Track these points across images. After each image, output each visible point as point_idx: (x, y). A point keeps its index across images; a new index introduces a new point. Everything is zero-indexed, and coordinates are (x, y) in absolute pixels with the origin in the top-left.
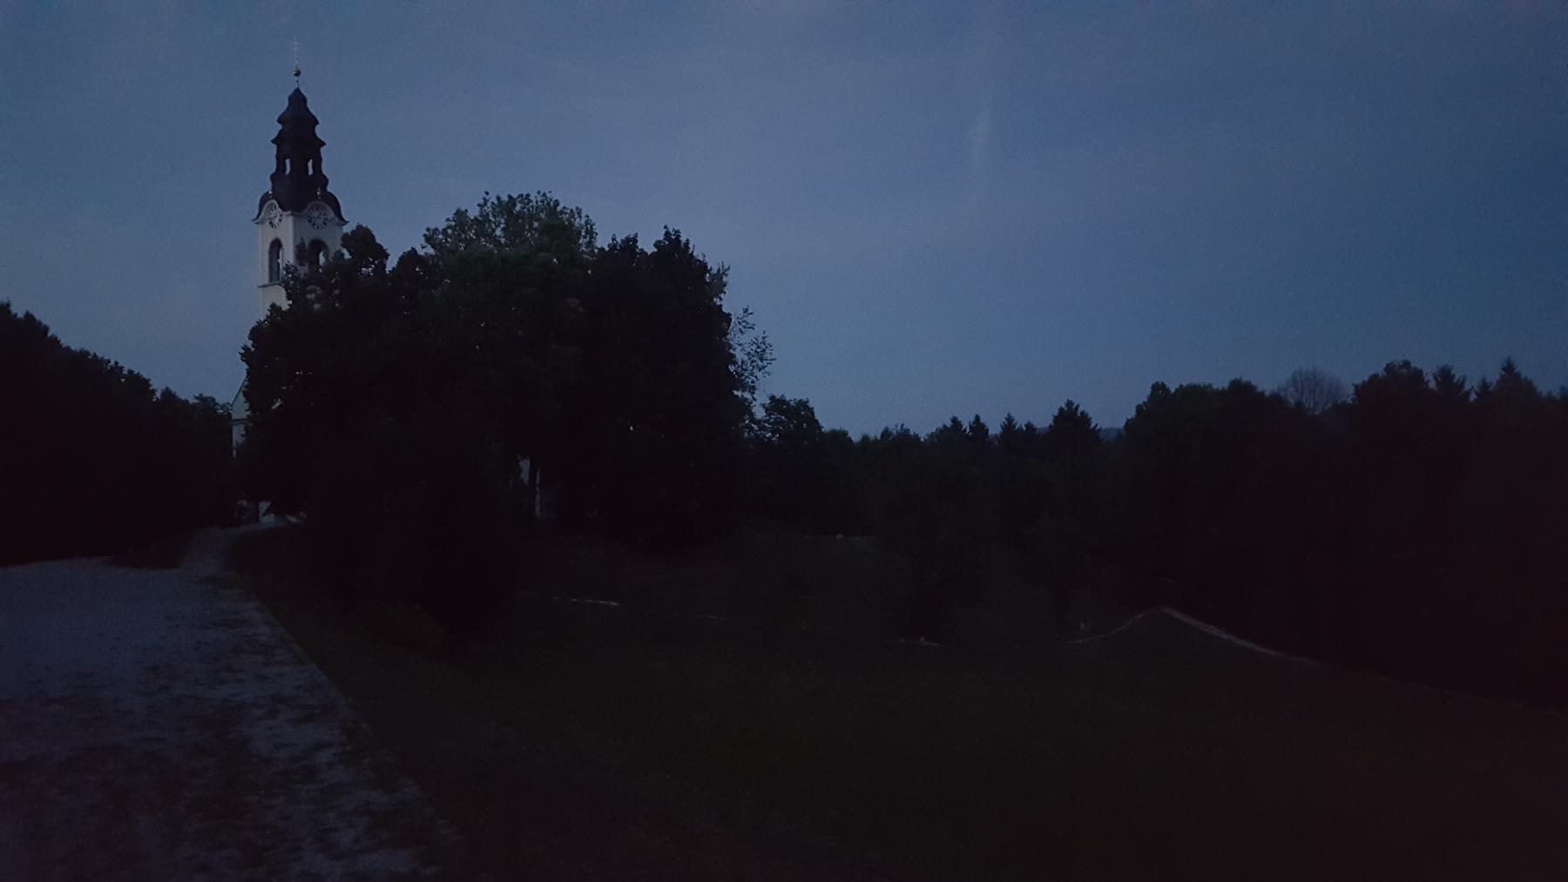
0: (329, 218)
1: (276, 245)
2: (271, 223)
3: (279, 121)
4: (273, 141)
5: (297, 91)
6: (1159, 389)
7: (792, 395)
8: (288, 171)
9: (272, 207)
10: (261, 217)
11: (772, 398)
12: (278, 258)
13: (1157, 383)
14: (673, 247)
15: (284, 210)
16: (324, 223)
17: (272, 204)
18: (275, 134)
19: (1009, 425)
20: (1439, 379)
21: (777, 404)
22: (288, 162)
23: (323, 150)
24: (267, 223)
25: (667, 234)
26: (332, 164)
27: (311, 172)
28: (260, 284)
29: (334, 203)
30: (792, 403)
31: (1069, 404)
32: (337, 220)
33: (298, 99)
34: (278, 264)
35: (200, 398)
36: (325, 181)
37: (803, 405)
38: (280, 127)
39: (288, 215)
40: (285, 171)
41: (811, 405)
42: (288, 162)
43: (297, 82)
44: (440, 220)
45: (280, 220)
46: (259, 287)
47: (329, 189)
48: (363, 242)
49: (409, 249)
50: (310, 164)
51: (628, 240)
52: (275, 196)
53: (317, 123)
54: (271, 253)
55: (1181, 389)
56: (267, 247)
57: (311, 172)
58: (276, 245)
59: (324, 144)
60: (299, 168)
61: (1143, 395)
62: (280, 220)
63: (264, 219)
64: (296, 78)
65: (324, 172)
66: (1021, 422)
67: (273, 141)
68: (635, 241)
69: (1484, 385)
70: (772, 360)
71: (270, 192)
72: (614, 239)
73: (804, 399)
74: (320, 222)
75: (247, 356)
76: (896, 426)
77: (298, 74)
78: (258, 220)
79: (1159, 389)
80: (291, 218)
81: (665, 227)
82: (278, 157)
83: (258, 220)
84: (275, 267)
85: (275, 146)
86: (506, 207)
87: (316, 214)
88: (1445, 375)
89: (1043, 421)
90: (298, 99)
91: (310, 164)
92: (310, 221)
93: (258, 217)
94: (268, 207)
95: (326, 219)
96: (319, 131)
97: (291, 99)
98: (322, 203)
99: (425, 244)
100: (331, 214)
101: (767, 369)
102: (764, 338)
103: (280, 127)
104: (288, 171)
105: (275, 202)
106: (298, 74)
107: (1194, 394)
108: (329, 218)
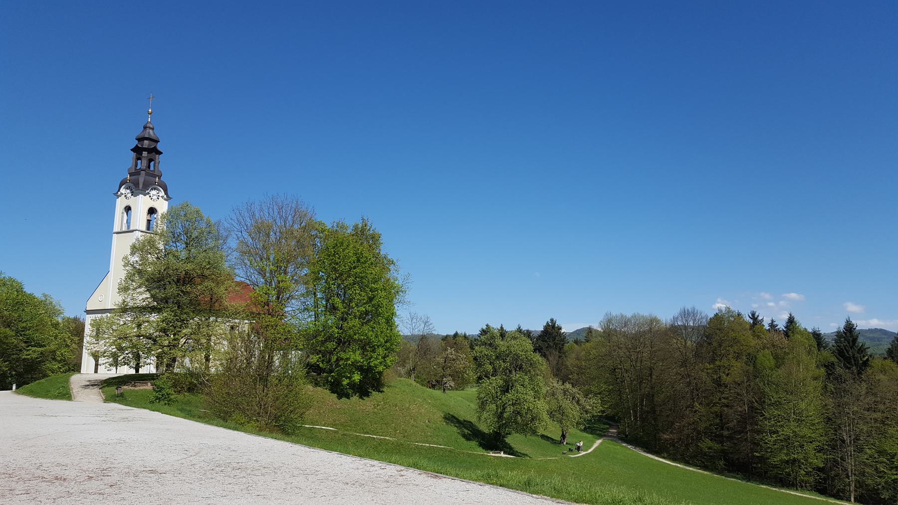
2: (125, 196)
3: (136, 139)
4: (132, 150)
10: (119, 193)
16: (158, 198)
18: (133, 146)
19: (519, 330)
20: (751, 316)
26: (163, 164)
27: (152, 168)
28: (116, 229)
31: (552, 320)
32: (165, 196)
40: (136, 166)
45: (132, 195)
46: (114, 233)
47: (162, 179)
50: (152, 164)
58: (128, 209)
59: (161, 153)
65: (162, 167)
66: (524, 328)
67: (132, 150)
69: (773, 321)
74: (155, 197)
87: (154, 192)
88: (754, 316)
89: (538, 327)
92: (150, 196)
95: (159, 196)
96: (159, 147)
97: (145, 128)
100: (163, 193)
105: (131, 185)
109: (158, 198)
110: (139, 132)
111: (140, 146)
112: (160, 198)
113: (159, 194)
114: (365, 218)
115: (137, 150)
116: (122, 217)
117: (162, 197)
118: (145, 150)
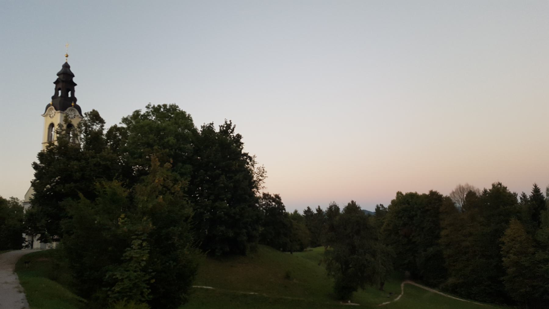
0: (76, 115)
1: (52, 125)
2: (50, 116)
3: (58, 75)
4: (55, 83)
5: (66, 63)
6: (399, 194)
7: (272, 194)
8: (60, 94)
9: (51, 109)
10: (46, 114)
11: (264, 194)
12: (52, 131)
13: (399, 192)
14: (227, 128)
15: (56, 109)
17: (52, 108)
18: (55, 80)
21: (266, 196)
22: (60, 92)
23: (76, 87)
24: (48, 116)
25: (226, 122)
26: (79, 92)
27: (70, 96)
29: (79, 109)
30: (272, 196)
32: (80, 116)
33: (66, 66)
34: (52, 134)
35: (12, 198)
36: (74, 99)
37: (277, 196)
38: (58, 77)
39: (58, 113)
41: (280, 196)
42: (60, 92)
43: (67, 59)
44: (129, 113)
45: (54, 115)
47: (77, 103)
48: (95, 117)
49: (114, 125)
50: (70, 93)
51: (210, 124)
52: (53, 105)
53: (74, 76)
54: (49, 129)
55: (406, 194)
56: (47, 126)
57: (70, 96)
59: (76, 85)
60: (65, 94)
61: (394, 197)
62: (54, 115)
63: (47, 114)
64: (66, 58)
65: (76, 95)
67: (55, 83)
68: (213, 124)
70: (266, 177)
71: (51, 103)
72: (204, 124)
73: (277, 193)
75: (35, 166)
76: (331, 202)
77: (67, 56)
78: (45, 115)
79: (399, 194)
80: (59, 114)
81: (225, 119)
82: (56, 89)
83: (45, 115)
84: (50, 135)
85: (54, 86)
86: (156, 110)
90: (66, 66)
91: (70, 93)
93: (44, 114)
94: (49, 110)
95: (75, 115)
96: (75, 80)
98: (74, 109)
99: (121, 122)
100: (77, 113)
101: (263, 181)
102: (263, 167)
103: (58, 77)
104: (60, 94)
105: (53, 107)
106: (67, 56)
107: (412, 196)
108: (76, 115)
109: (74, 117)
110: (60, 68)
111: (59, 80)
112: (76, 117)
113: (75, 114)
114: (229, 123)
115: (56, 83)
116: (54, 137)
117: (78, 116)
118: (63, 81)
